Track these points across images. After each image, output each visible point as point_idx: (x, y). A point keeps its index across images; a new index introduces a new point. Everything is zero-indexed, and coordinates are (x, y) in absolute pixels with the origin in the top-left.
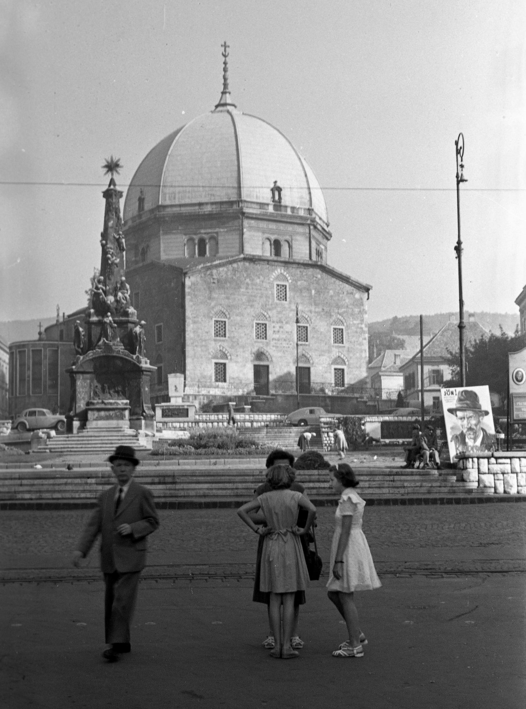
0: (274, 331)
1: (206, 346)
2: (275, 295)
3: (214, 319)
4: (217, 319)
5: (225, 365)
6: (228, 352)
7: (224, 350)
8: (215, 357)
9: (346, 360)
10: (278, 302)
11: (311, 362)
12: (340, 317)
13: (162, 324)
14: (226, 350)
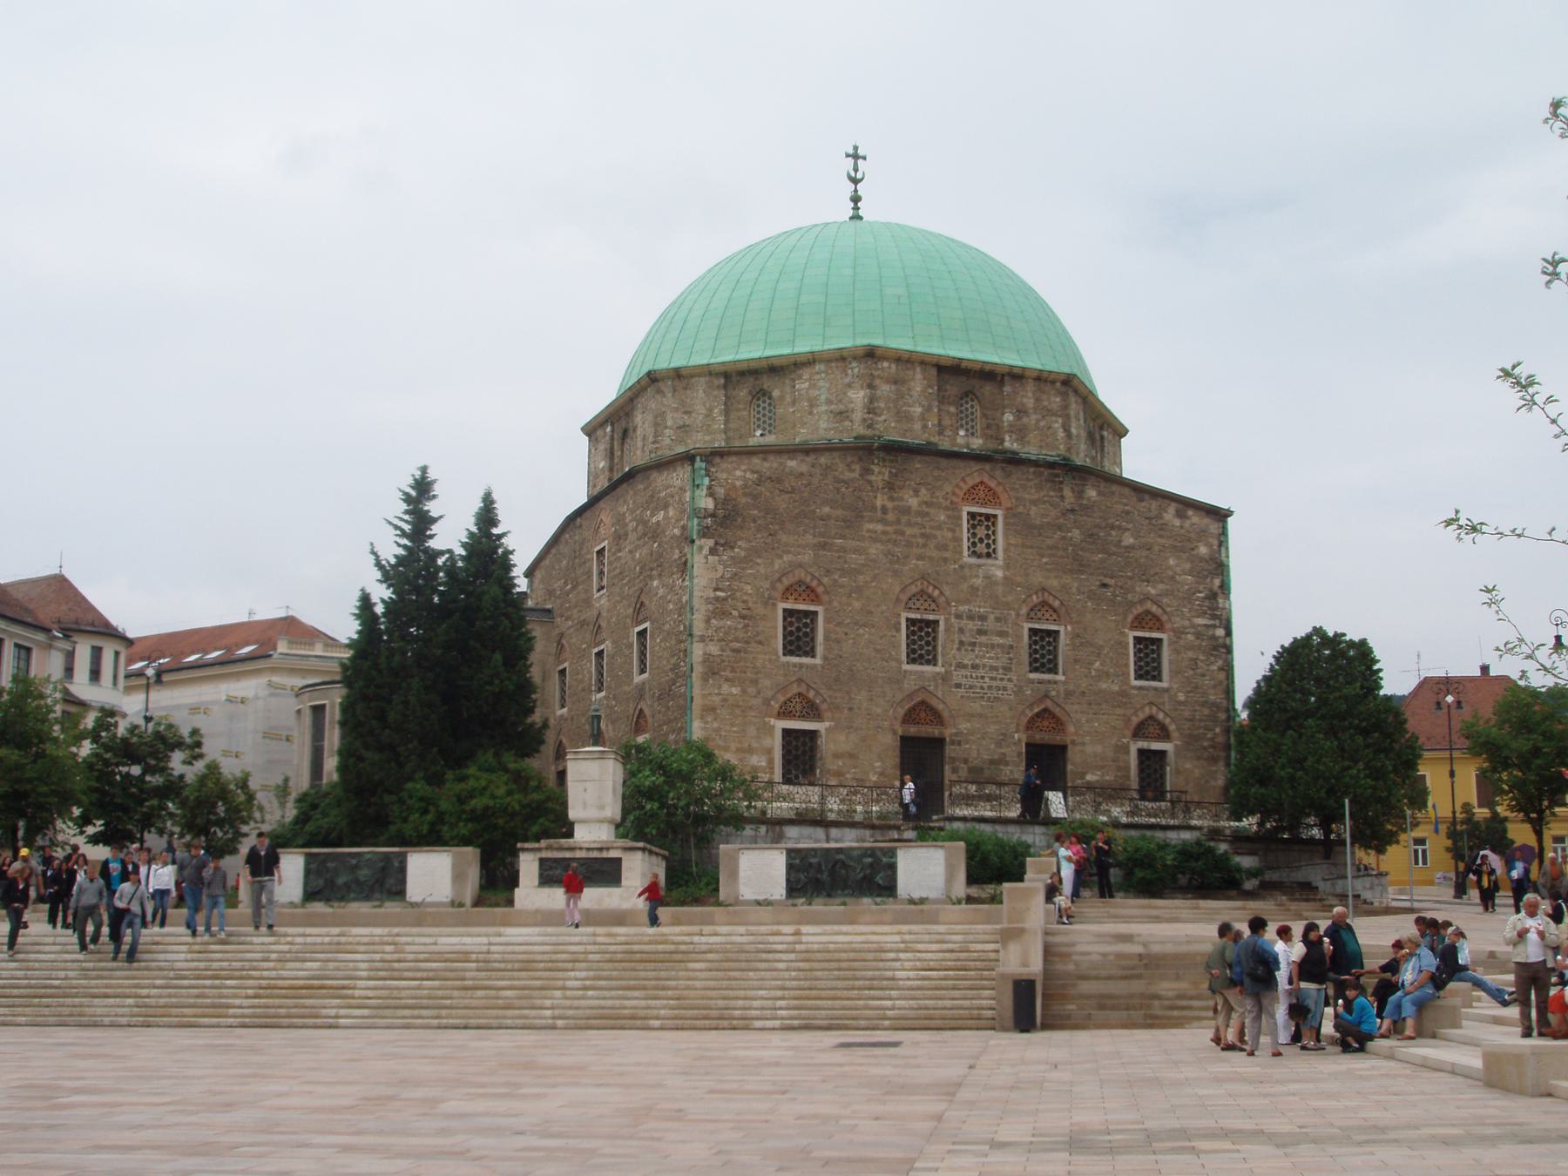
0: (961, 643)
1: (755, 682)
2: (965, 540)
3: (782, 606)
4: (788, 606)
5: (813, 734)
6: (825, 700)
7: (811, 694)
8: (784, 713)
9: (1172, 727)
10: (973, 560)
11: (1071, 729)
12: (1154, 609)
13: (646, 625)
14: (818, 693)
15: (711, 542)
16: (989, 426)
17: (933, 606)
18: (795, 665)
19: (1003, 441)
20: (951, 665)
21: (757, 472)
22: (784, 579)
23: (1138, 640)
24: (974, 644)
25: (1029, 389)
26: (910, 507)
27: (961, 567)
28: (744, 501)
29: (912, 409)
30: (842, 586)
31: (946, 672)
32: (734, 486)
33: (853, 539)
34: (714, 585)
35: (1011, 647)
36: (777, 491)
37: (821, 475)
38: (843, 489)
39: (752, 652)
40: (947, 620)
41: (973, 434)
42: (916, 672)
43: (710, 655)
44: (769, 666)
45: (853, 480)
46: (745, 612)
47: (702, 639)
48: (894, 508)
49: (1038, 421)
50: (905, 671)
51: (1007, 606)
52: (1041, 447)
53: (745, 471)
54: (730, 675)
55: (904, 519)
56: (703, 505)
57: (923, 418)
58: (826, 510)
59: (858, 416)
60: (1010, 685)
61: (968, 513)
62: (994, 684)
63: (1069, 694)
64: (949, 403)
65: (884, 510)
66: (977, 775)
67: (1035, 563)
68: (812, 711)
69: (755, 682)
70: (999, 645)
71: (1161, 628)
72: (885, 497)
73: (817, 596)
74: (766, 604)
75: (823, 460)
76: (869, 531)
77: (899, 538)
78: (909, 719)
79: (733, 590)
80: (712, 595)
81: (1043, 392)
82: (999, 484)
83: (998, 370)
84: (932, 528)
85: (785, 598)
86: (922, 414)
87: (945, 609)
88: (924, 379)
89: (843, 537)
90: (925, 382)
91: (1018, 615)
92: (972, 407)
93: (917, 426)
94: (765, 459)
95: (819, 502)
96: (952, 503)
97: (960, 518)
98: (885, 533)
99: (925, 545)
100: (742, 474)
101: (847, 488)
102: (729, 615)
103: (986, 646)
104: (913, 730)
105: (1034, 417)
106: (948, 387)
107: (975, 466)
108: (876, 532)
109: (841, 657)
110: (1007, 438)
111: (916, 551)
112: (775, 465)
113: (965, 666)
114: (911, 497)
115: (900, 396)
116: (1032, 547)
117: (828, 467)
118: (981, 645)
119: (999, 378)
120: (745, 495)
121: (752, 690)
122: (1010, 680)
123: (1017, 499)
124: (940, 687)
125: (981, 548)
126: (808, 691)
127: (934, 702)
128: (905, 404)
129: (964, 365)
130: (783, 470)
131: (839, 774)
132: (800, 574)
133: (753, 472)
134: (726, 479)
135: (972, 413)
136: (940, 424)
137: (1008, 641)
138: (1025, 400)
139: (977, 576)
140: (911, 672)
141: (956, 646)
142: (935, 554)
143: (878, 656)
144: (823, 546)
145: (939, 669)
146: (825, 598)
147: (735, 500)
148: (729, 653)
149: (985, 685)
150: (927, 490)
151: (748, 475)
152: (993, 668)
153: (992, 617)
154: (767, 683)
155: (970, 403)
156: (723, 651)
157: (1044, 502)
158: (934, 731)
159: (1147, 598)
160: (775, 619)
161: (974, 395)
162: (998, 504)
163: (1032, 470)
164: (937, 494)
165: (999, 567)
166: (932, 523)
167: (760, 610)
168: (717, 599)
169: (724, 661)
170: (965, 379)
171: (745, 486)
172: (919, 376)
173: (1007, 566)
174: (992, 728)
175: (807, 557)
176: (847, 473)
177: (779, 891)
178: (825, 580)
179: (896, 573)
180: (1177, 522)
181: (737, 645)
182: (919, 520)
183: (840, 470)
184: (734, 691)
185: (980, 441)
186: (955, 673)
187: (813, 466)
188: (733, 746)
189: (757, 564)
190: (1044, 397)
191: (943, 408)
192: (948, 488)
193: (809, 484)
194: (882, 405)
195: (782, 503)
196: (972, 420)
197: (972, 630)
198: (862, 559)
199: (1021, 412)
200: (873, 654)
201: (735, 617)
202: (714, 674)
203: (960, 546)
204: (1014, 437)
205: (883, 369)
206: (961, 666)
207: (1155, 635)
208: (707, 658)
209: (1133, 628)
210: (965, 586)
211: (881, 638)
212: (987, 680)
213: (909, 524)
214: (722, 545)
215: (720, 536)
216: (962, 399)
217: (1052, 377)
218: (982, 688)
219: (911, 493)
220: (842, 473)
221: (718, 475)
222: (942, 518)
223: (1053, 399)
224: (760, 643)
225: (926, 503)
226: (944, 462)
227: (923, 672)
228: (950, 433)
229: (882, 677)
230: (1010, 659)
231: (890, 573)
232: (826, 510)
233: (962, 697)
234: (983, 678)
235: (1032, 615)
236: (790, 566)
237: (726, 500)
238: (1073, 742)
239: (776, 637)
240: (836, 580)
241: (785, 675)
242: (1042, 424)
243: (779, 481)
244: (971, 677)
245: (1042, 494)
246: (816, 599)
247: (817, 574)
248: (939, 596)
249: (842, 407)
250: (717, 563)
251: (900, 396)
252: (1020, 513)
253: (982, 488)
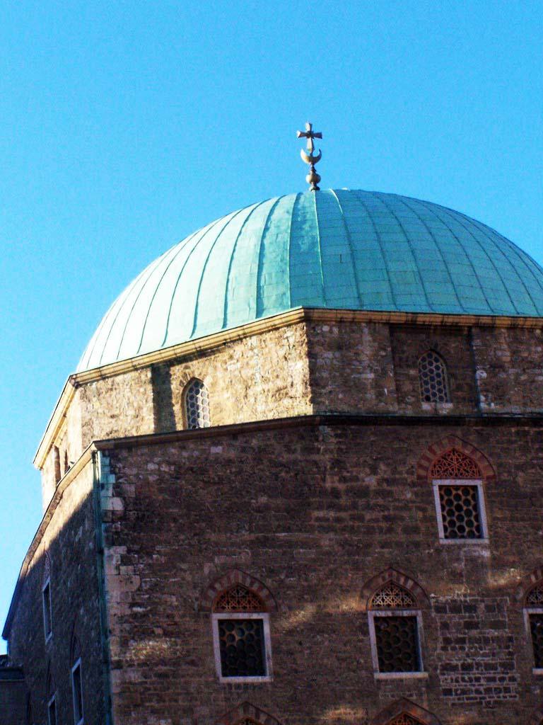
0: (447, 641)
1: (189, 711)
2: (440, 519)
10: (450, 542)
15: (122, 550)
16: (459, 387)
17: (408, 600)
18: (238, 686)
19: (478, 402)
20: (436, 669)
21: (174, 464)
22: (217, 586)
24: (462, 641)
25: (502, 340)
26: (368, 487)
27: (439, 551)
28: (160, 498)
29: (364, 376)
30: (289, 588)
31: (430, 676)
33: (300, 531)
34: (130, 600)
35: (510, 639)
36: (201, 484)
37: (254, 459)
38: (283, 474)
39: (183, 676)
40: (425, 616)
41: (441, 399)
42: (393, 681)
43: (130, 683)
44: (206, 690)
45: (295, 462)
46: (170, 628)
48: (347, 491)
49: (518, 375)
50: (379, 681)
52: (525, 405)
53: (159, 464)
54: (155, 704)
55: (361, 502)
56: (110, 507)
57: (377, 385)
58: (263, 499)
59: (299, 389)
60: (513, 686)
61: (441, 487)
62: (492, 685)
64: (408, 366)
65: (335, 493)
67: (530, 537)
69: (189, 711)
70: (494, 639)
72: (336, 478)
73: (261, 602)
75: (254, 442)
76: (318, 519)
77: (357, 524)
79: (155, 603)
80: (128, 612)
81: (521, 343)
82: (475, 450)
83: (462, 321)
84: (396, 508)
85: (220, 609)
86: (375, 380)
87: (422, 602)
88: (374, 341)
89: (288, 530)
90: (376, 344)
91: (514, 600)
92: (437, 368)
93: (371, 395)
94: (183, 448)
95: (253, 491)
96: (419, 477)
97: (431, 493)
98: (338, 520)
99: (390, 530)
100: (157, 467)
101: (287, 472)
103: (478, 641)
105: (511, 371)
106: (405, 348)
107: (443, 433)
108: (328, 520)
109: (296, 671)
110: (482, 398)
111: (378, 537)
112: (196, 453)
113: (454, 668)
114: (368, 475)
115: (346, 363)
116: (523, 519)
117: (262, 451)
118: (473, 640)
119: (465, 333)
120: (161, 491)
122: (512, 679)
123: (500, 465)
124: (425, 697)
126: (258, 716)
128: (353, 370)
129: (420, 319)
130: (207, 459)
132: (236, 577)
133: (169, 463)
134: (137, 476)
135: (438, 375)
136: (398, 389)
137: (506, 632)
138: (499, 353)
139: (458, 560)
140: (386, 681)
141: (440, 645)
142: (403, 538)
143: (344, 665)
144: (264, 542)
145: (419, 675)
146: (270, 603)
147: (149, 497)
148: (154, 679)
149: (482, 689)
150: (388, 465)
151: (164, 468)
152: (489, 667)
153: (482, 605)
154: (205, 711)
155: (435, 364)
156: (145, 677)
157: (533, 466)
160: (209, 633)
161: (438, 353)
162: (477, 474)
163: (513, 430)
164: (400, 469)
165: (484, 547)
166: (397, 504)
167: (189, 623)
168: (135, 615)
169: (149, 689)
170: (424, 336)
171: (161, 480)
172: (367, 338)
173: (494, 545)
175: (244, 557)
176: (286, 456)
178: (269, 582)
179: (357, 567)
182: (380, 501)
183: (276, 452)
185: (450, 405)
186: (442, 677)
187: (243, 450)
189: (181, 569)
190: (522, 347)
191: (400, 371)
192: (412, 461)
193: (239, 473)
194: (325, 375)
195: (206, 496)
196: (439, 383)
197: (459, 624)
198: (312, 554)
199: (496, 367)
200: (337, 664)
201: (159, 636)
202: (136, 706)
203: (435, 526)
204: (490, 395)
205: (323, 334)
206: (448, 668)
208: (126, 686)
211: (345, 645)
212: (482, 682)
213: (368, 507)
214: (137, 552)
215: (134, 541)
216: (424, 360)
217: (529, 323)
218: (478, 692)
219: (368, 470)
220: (279, 455)
221: (127, 471)
222: (409, 496)
223: (533, 349)
224: (193, 663)
225: (387, 481)
226: (404, 431)
227: (401, 680)
228: (413, 399)
229: (350, 691)
230: (510, 654)
231: (348, 566)
232: (263, 499)
233: (453, 705)
234: (478, 679)
235: (532, 599)
236: (223, 569)
237: (137, 501)
239: (212, 654)
240: (282, 581)
241: (227, 699)
242: (523, 378)
243: (203, 471)
244: (463, 680)
245: (529, 456)
246: (260, 607)
247: (258, 576)
248: (413, 588)
249: (280, 383)
250: (131, 573)
251: (346, 363)
252: (505, 481)
253: (454, 458)
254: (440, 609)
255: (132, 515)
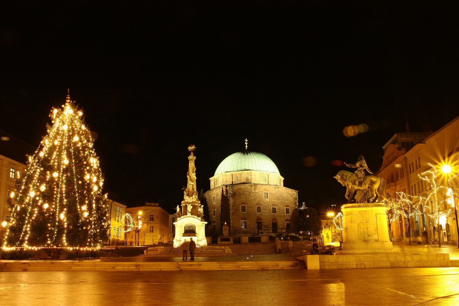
2: (264, 197)
3: (241, 205)
11: (278, 220)
15: (232, 197)
23: (286, 209)
32: (235, 190)
47: (232, 210)
51: (269, 204)
54: (235, 214)
63: (277, 216)
65: (254, 192)
66: (266, 227)
68: (246, 219)
69: (238, 215)
71: (289, 207)
74: (239, 205)
78: (256, 220)
102: (235, 207)
104: (258, 221)
121: (238, 216)
125: (266, 197)
127: (260, 217)
131: (249, 227)
137: (270, 209)
158: (260, 221)
159: (287, 203)
167: (238, 206)
173: (269, 199)
174: (268, 221)
177: (247, 242)
180: (291, 193)
181: (236, 211)
184: (236, 216)
188: (236, 224)
206: (263, 213)
207: (288, 208)
208: (232, 212)
209: (285, 207)
210: (264, 202)
213: (257, 194)
238: (278, 222)
254: (263, 206)
255: (233, 193)
